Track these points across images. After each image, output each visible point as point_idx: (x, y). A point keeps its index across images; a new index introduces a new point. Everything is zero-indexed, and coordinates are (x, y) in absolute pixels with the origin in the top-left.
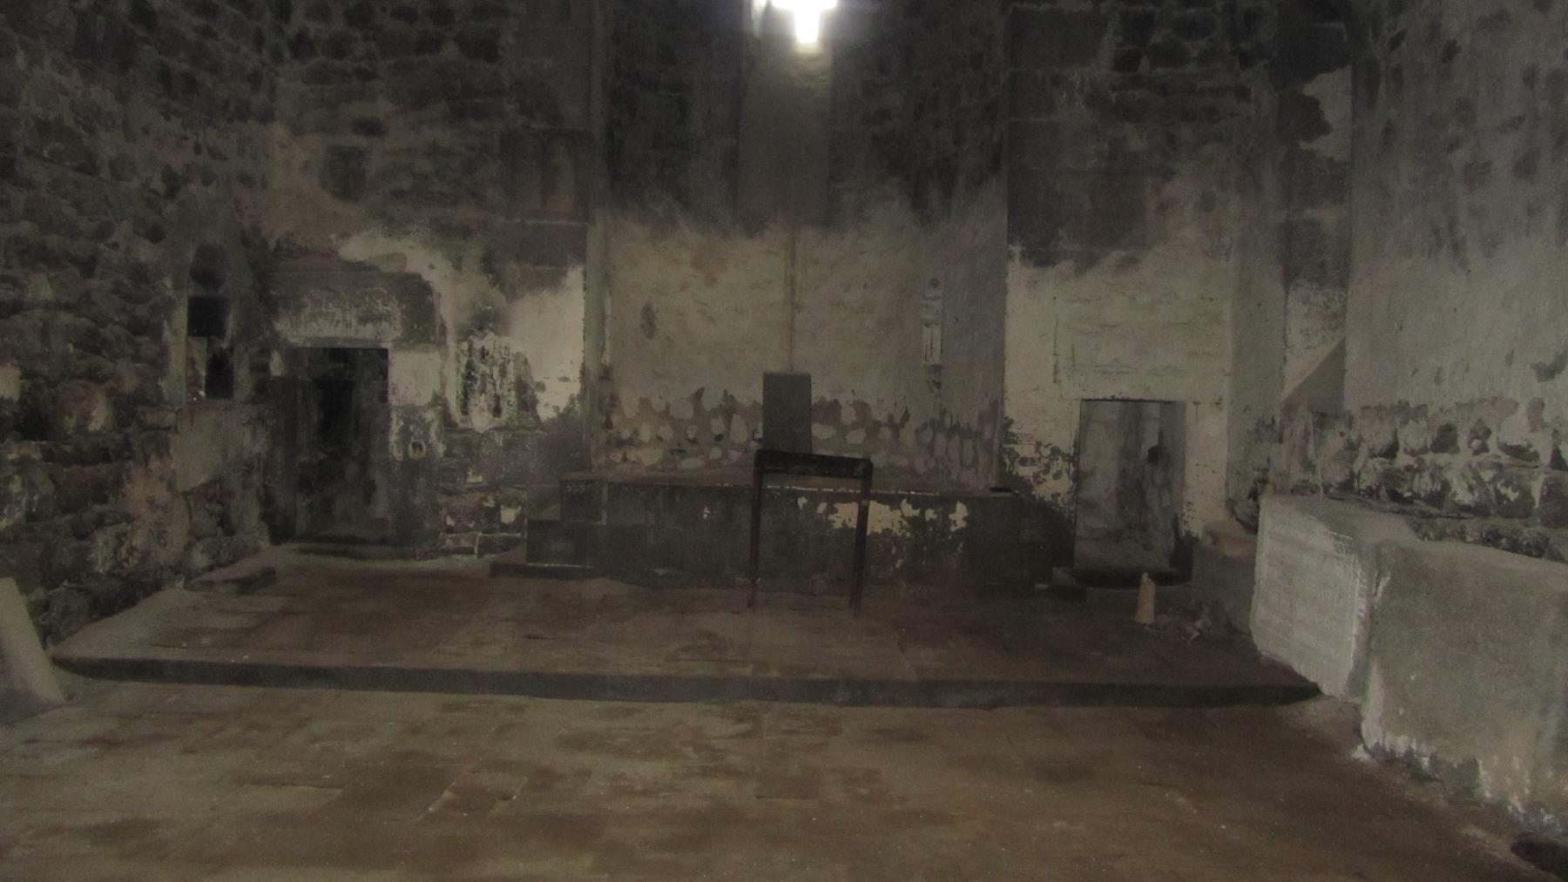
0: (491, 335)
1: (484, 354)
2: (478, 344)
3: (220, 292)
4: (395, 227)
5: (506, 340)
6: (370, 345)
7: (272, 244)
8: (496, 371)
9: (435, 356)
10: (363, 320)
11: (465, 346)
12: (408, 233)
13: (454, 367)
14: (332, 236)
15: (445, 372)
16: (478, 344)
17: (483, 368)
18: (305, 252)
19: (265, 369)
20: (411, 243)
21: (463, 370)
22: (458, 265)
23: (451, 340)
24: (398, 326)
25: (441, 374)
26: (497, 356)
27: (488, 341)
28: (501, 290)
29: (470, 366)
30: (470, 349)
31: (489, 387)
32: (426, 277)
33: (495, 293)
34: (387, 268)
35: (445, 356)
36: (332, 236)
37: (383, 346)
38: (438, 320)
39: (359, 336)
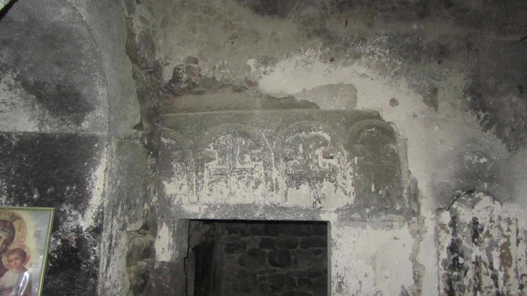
0: (486, 200)
1: (476, 230)
2: (466, 216)
3: (85, 125)
4: (337, 49)
5: (512, 210)
6: (302, 217)
7: (167, 75)
8: (496, 254)
9: (404, 232)
10: (296, 180)
11: (446, 217)
12: (357, 56)
13: (434, 251)
14: (251, 62)
15: (421, 258)
16: (466, 216)
17: (476, 252)
18: (211, 85)
19: (148, 252)
20: (362, 70)
21: (444, 255)
22: (431, 98)
23: (426, 212)
24: (350, 189)
25: (413, 260)
26: (495, 233)
27: (483, 209)
28: (499, 134)
29: (454, 248)
30: (454, 223)
31: (487, 281)
32: (386, 117)
33: (489, 139)
34: (327, 104)
35: (418, 234)
36: (251, 62)
37: (323, 217)
38: (406, 182)
39: (289, 203)
